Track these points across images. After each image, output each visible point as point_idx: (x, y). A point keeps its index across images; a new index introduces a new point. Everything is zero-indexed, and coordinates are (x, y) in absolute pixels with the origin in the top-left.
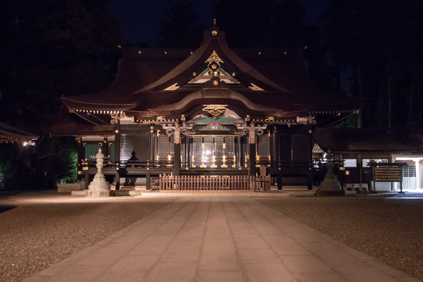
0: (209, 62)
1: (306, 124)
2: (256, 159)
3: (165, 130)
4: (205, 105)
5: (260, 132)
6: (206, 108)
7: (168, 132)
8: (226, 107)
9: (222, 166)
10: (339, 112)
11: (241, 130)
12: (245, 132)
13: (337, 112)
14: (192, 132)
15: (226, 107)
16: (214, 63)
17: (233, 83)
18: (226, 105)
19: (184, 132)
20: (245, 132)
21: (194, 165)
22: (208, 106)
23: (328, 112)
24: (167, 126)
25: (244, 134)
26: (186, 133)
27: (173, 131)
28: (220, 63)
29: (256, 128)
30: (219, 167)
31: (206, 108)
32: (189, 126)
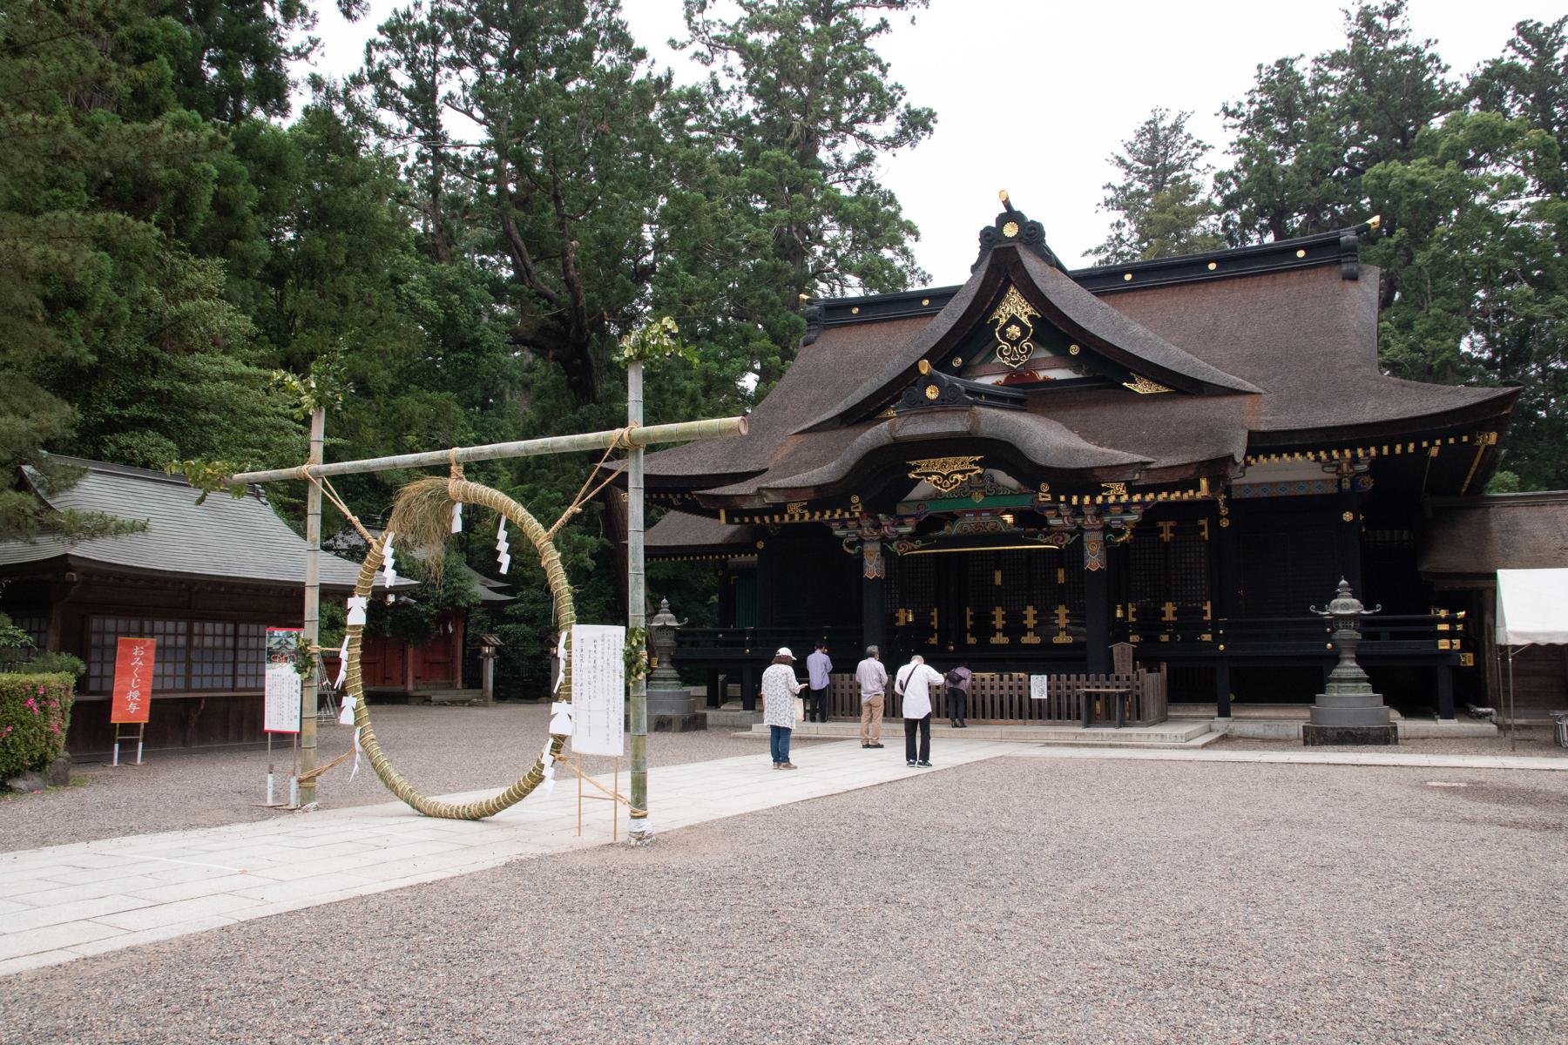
0: (997, 320)
1: (1335, 490)
2: (1164, 614)
3: (841, 539)
4: (913, 463)
5: (1120, 533)
6: (918, 471)
7: (848, 545)
8: (975, 463)
9: (994, 640)
10: (1432, 444)
11: (1060, 531)
12: (1072, 533)
13: (1425, 444)
14: (914, 541)
15: (975, 463)
16: (1013, 320)
17: (1080, 376)
18: (977, 458)
19: (891, 542)
20: (1072, 533)
21: (972, 636)
22: (923, 463)
23: (1379, 449)
24: (844, 527)
25: (1069, 539)
26: (895, 545)
27: (861, 541)
28: (1031, 318)
29: (1107, 519)
30: (1015, 643)
31: (918, 471)
32: (902, 524)
